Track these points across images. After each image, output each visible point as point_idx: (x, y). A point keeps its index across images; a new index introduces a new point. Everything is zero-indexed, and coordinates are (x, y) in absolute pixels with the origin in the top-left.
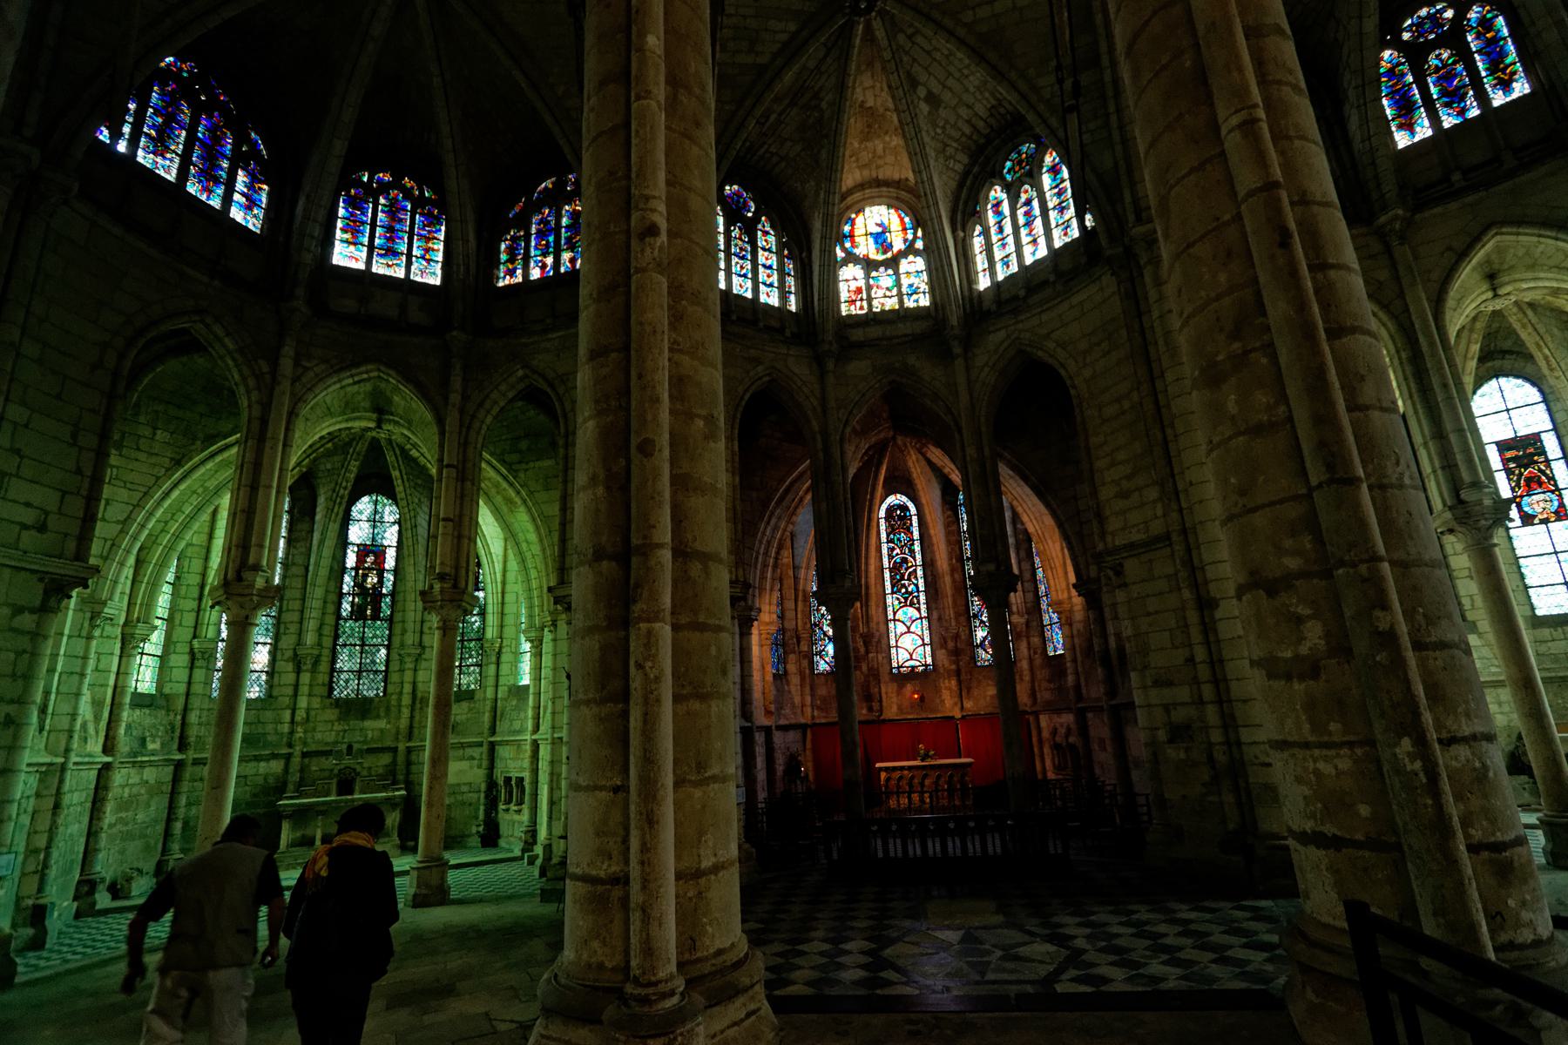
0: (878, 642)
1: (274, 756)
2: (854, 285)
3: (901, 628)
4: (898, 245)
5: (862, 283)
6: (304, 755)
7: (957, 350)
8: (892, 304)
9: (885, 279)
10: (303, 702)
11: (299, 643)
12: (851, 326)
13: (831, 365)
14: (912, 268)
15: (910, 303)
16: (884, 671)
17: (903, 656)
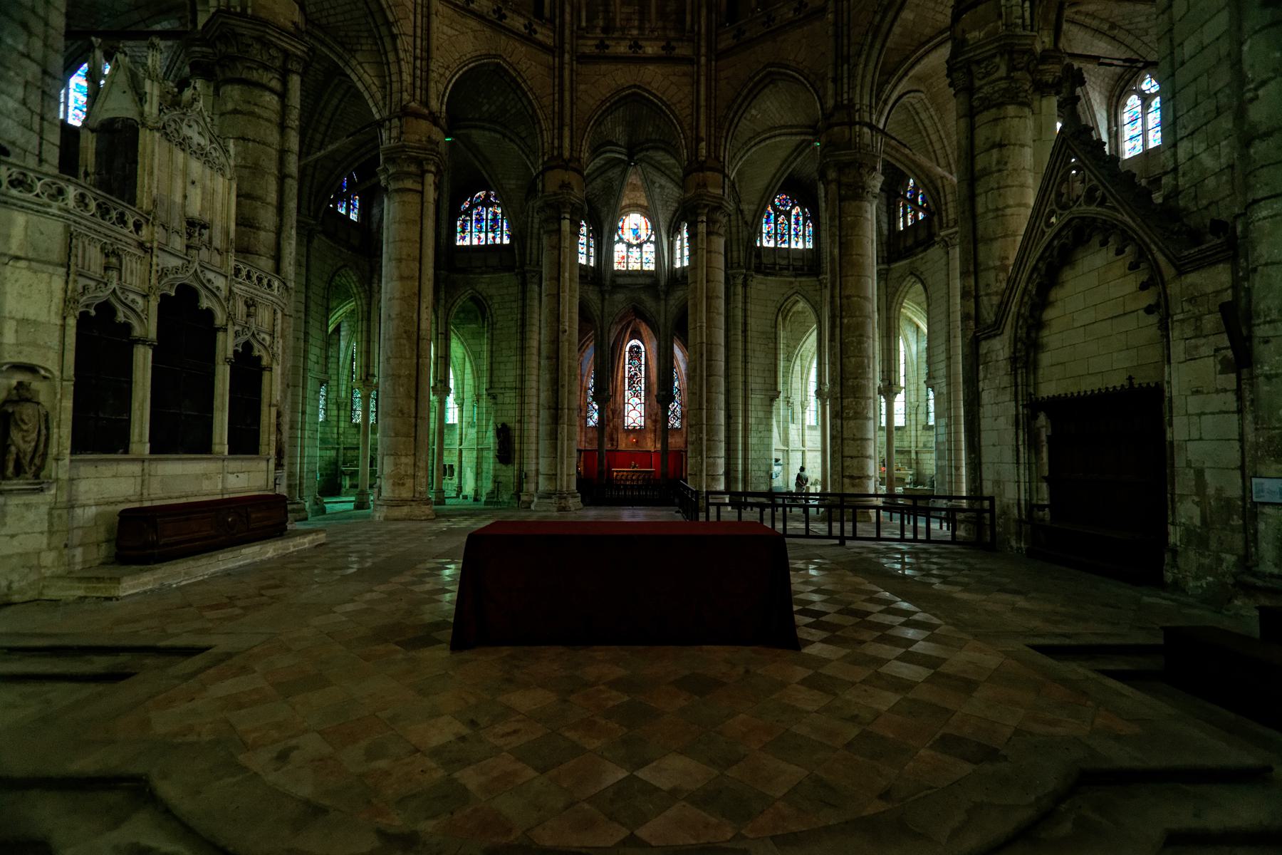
0: (619, 414)
1: (333, 448)
2: (621, 255)
3: (632, 408)
4: (644, 237)
5: (625, 254)
6: (345, 449)
7: (663, 296)
8: (637, 267)
9: (635, 252)
10: (342, 424)
11: (338, 396)
12: (618, 276)
13: (607, 296)
14: (649, 250)
15: (645, 268)
16: (620, 428)
17: (631, 421)
